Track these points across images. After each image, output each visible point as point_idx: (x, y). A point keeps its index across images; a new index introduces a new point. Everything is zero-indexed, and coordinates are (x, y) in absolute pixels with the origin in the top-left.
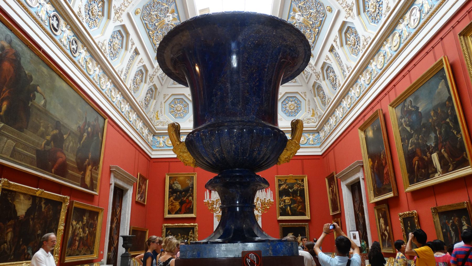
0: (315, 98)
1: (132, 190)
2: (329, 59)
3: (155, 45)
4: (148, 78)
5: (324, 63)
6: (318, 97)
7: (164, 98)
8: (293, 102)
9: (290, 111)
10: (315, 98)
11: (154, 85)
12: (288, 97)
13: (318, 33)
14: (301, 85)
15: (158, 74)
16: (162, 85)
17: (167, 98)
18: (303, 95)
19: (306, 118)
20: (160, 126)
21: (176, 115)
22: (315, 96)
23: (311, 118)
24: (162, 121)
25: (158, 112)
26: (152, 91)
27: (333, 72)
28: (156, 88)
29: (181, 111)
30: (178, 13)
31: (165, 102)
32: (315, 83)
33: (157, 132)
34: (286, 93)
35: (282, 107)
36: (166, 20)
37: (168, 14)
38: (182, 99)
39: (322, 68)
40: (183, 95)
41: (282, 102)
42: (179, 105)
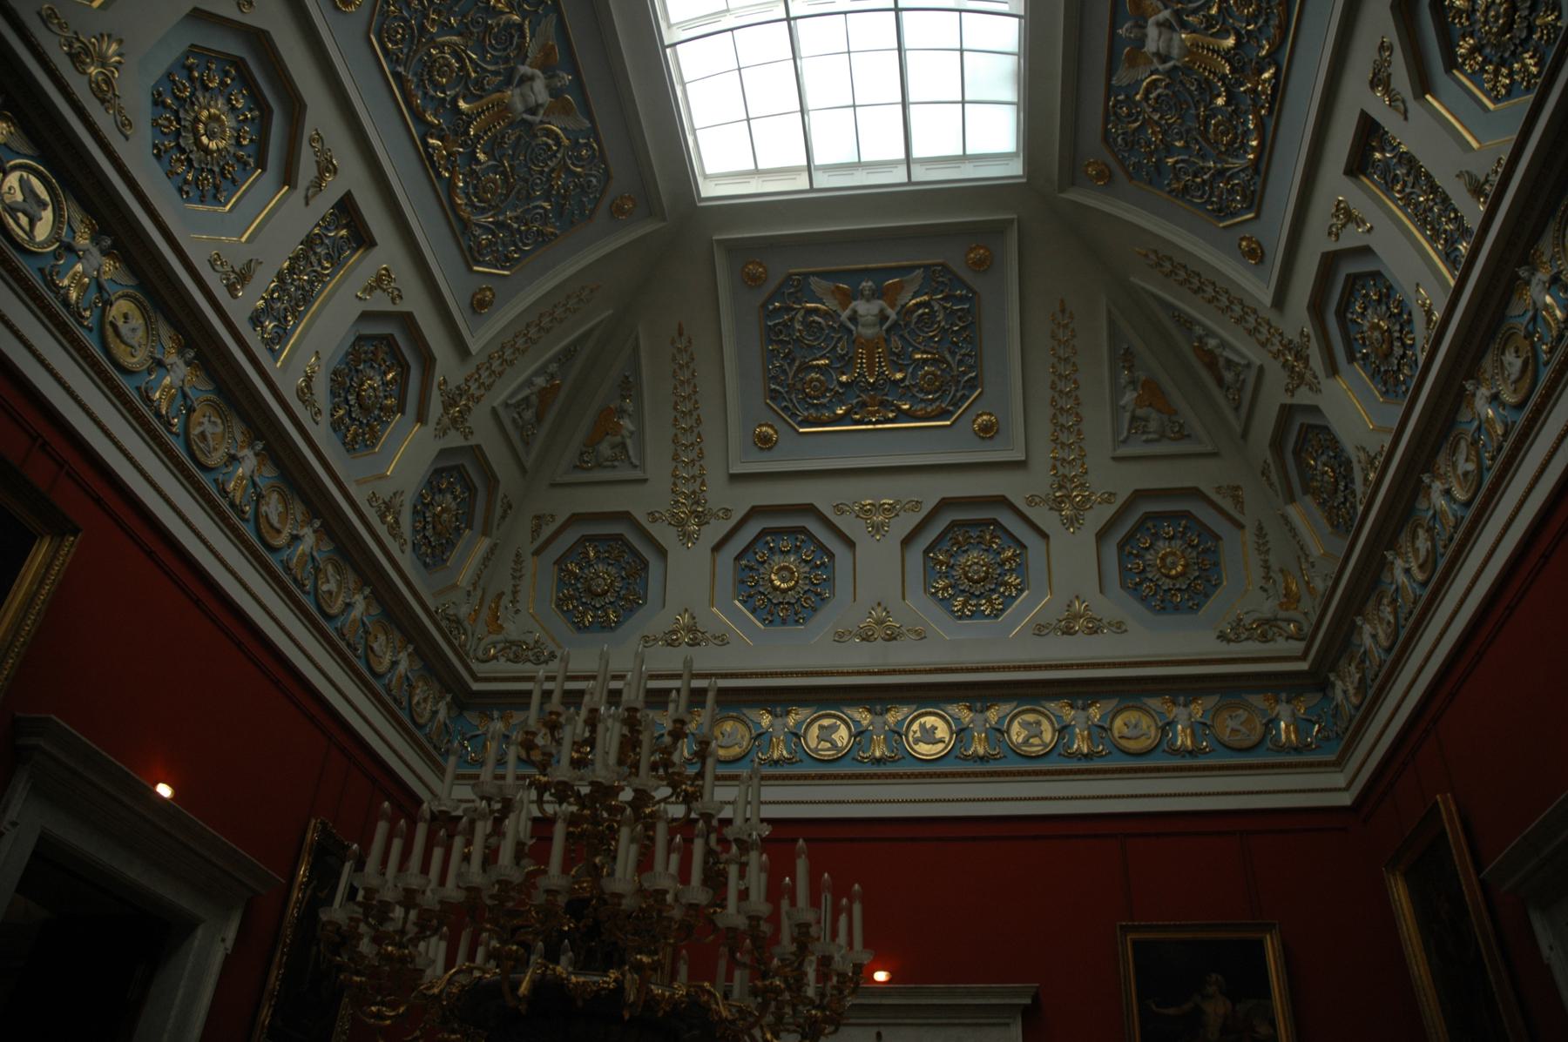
0: (1293, 511)
1: (231, 934)
2: (1349, 217)
3: (465, 225)
4: (435, 393)
5: (1330, 262)
6: (1308, 498)
7: (536, 532)
8: (1177, 544)
9: (1166, 584)
10: (1293, 511)
11: (476, 452)
12: (1148, 516)
13: (1279, 87)
14: (1209, 448)
15: (499, 396)
16: (523, 470)
17: (547, 531)
18: (1227, 504)
19: (1257, 615)
20: (503, 666)
21: (584, 614)
22: (1291, 499)
23: (1282, 614)
24: (514, 636)
25: (501, 595)
26: (470, 488)
27: (1387, 293)
28: (491, 480)
29: (610, 598)
30: (575, 71)
31: (537, 553)
32: (1287, 412)
33: (476, 686)
34: (1139, 495)
35: (1123, 570)
36: (512, 95)
37: (525, 69)
38: (619, 538)
39: (1317, 308)
40: (625, 517)
41: (1121, 547)
42: (601, 567)
